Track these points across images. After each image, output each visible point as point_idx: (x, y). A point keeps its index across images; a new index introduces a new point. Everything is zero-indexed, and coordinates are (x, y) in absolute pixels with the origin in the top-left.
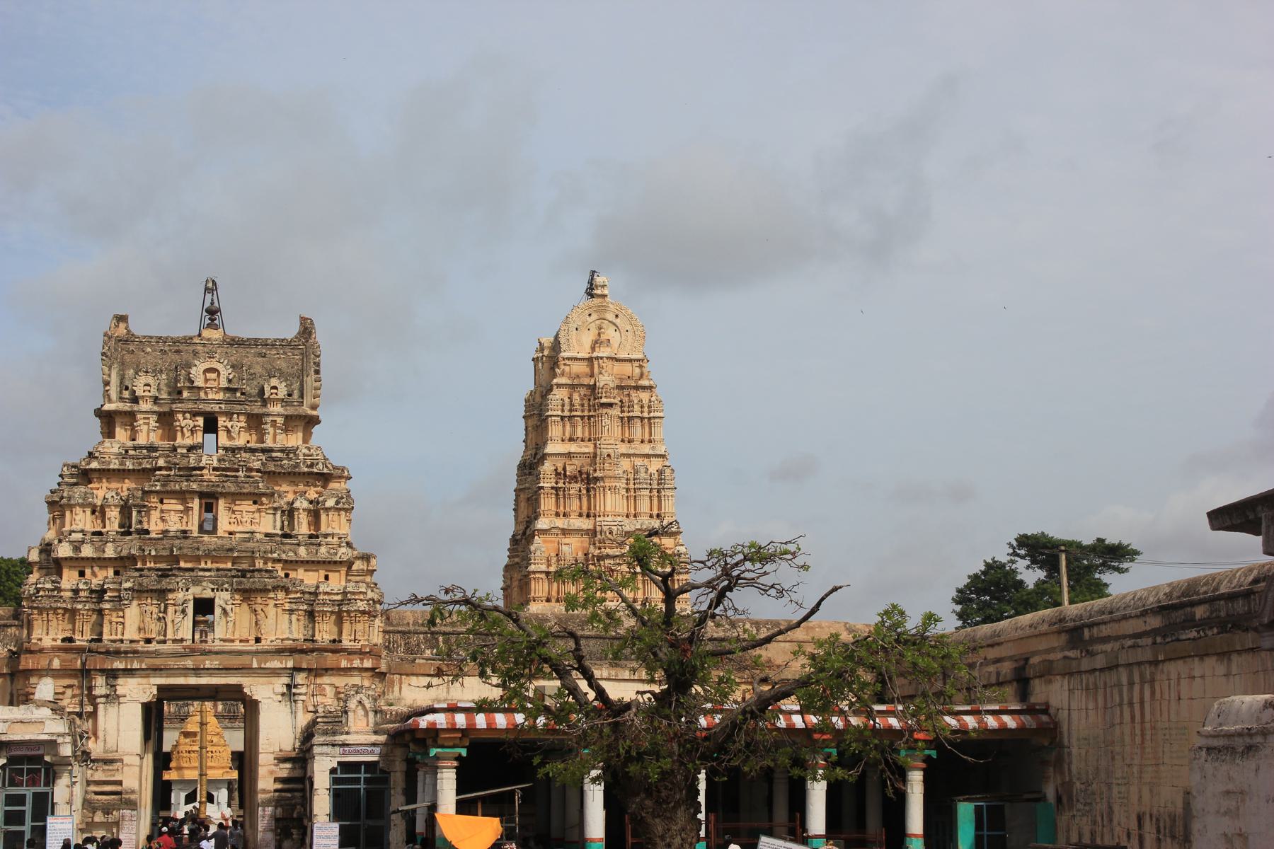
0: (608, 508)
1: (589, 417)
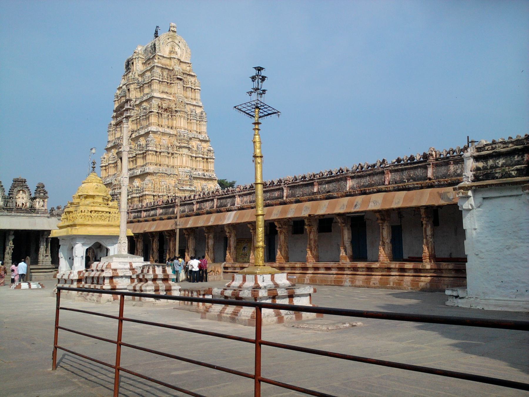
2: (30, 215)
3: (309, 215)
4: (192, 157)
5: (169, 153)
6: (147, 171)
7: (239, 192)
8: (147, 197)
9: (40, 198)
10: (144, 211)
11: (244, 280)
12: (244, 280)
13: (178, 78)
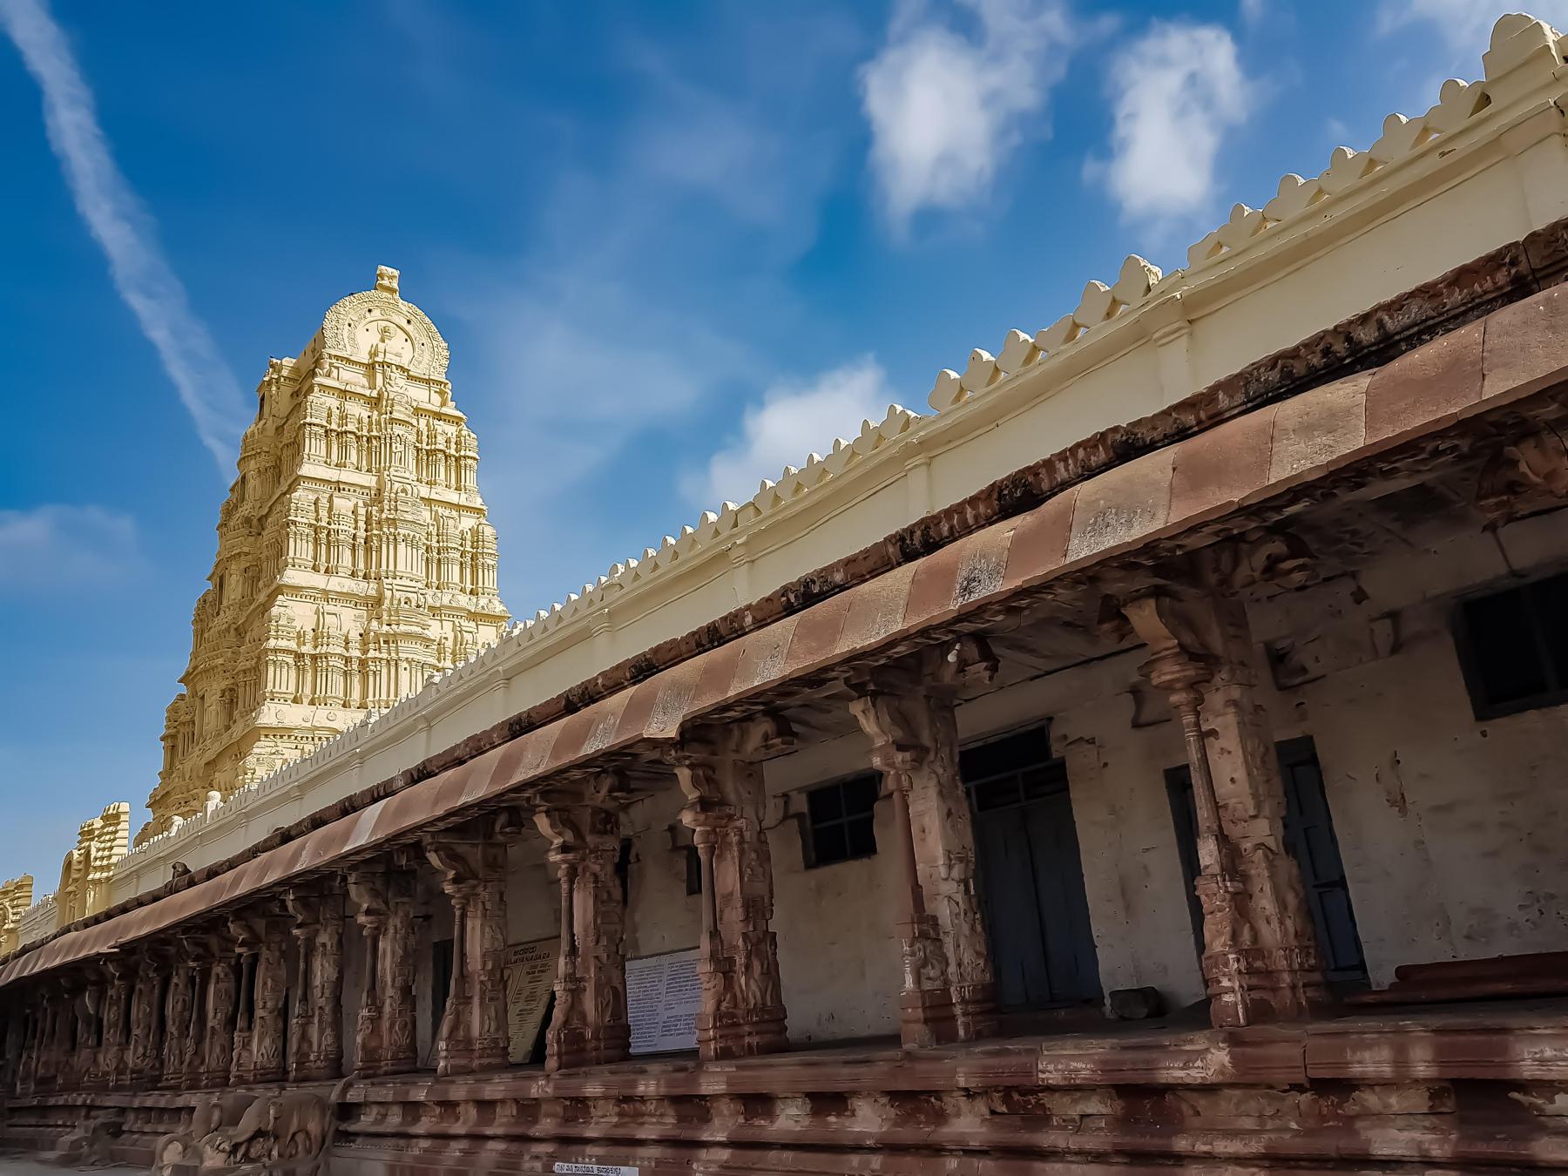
5: (348, 660)
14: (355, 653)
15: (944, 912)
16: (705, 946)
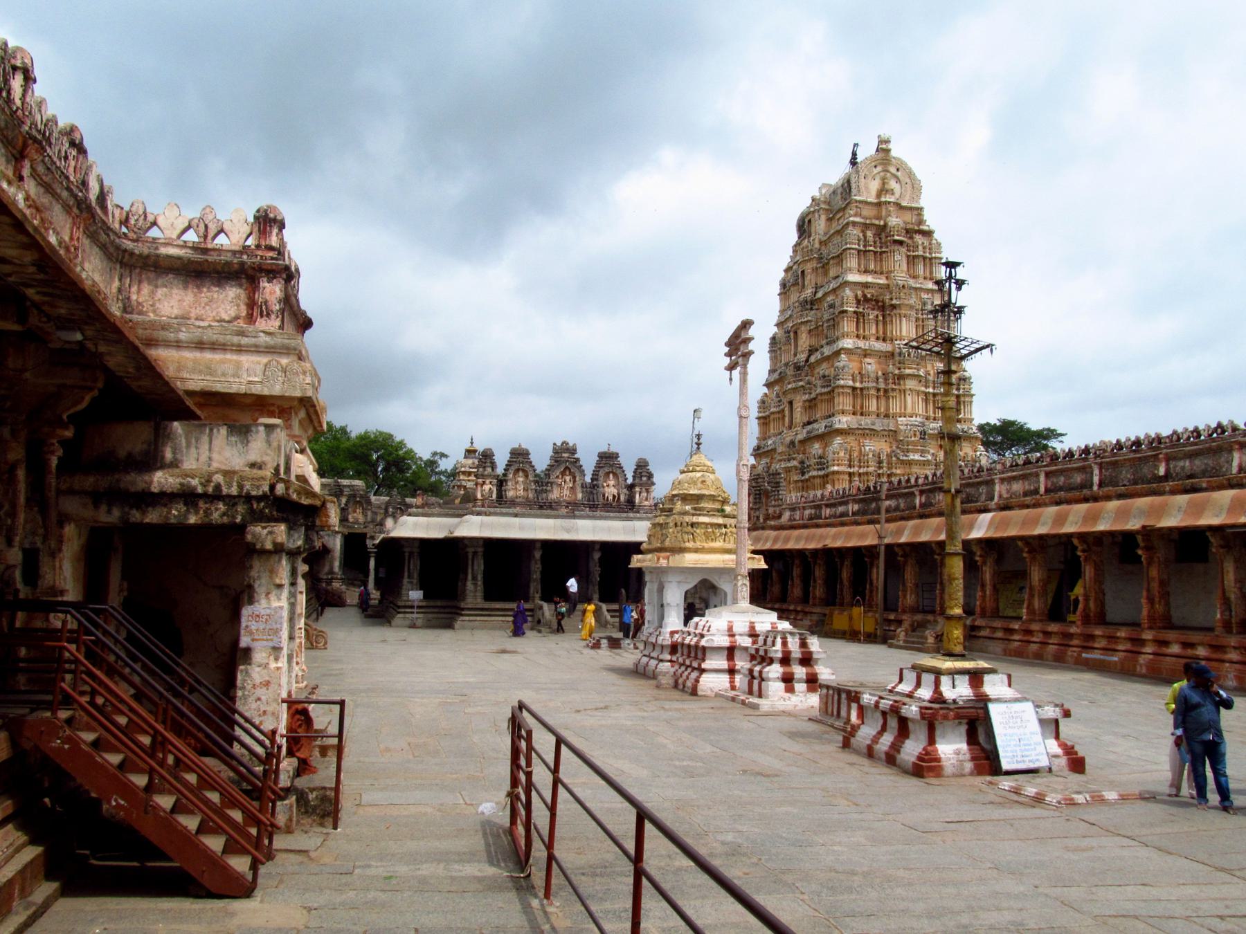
0: (904, 333)
1: (881, 253)
2: (624, 515)
3: (1144, 527)
4: (926, 394)
5: (878, 390)
6: (837, 426)
7: (1003, 472)
8: (837, 476)
9: (641, 485)
10: (827, 506)
11: (918, 685)
12: (918, 685)
13: (896, 242)
14: (882, 386)
15: (1232, 597)
16: (1144, 594)
